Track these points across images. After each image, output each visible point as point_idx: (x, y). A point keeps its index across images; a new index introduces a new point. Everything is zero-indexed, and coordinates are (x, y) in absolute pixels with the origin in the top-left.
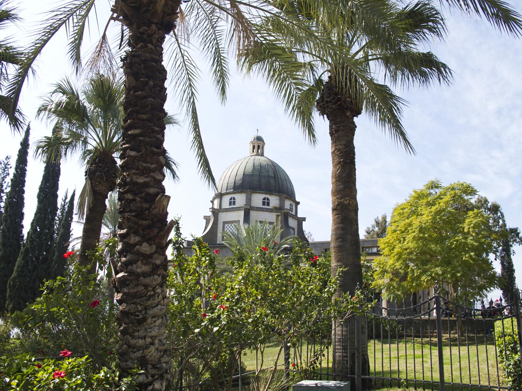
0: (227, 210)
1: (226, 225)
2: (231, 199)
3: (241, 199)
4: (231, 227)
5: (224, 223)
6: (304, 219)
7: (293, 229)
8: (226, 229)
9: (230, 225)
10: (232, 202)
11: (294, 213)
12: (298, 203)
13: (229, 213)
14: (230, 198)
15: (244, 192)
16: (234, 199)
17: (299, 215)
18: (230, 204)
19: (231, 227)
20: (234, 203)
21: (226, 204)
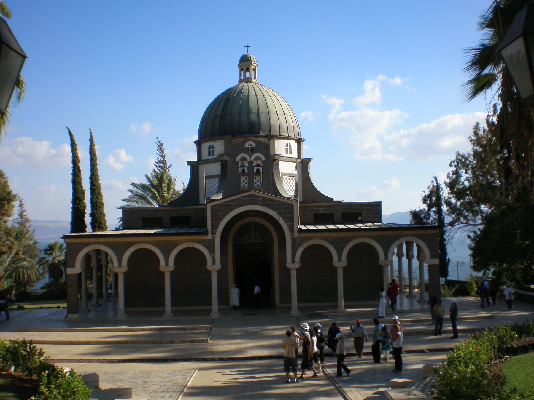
0: (208, 162)
2: (209, 148)
3: (219, 146)
4: (212, 183)
8: (208, 186)
9: (211, 181)
10: (211, 152)
11: (295, 154)
12: (299, 141)
14: (208, 146)
15: (222, 139)
16: (213, 147)
17: (304, 156)
18: (209, 155)
19: (212, 183)
20: (213, 154)
21: (205, 155)
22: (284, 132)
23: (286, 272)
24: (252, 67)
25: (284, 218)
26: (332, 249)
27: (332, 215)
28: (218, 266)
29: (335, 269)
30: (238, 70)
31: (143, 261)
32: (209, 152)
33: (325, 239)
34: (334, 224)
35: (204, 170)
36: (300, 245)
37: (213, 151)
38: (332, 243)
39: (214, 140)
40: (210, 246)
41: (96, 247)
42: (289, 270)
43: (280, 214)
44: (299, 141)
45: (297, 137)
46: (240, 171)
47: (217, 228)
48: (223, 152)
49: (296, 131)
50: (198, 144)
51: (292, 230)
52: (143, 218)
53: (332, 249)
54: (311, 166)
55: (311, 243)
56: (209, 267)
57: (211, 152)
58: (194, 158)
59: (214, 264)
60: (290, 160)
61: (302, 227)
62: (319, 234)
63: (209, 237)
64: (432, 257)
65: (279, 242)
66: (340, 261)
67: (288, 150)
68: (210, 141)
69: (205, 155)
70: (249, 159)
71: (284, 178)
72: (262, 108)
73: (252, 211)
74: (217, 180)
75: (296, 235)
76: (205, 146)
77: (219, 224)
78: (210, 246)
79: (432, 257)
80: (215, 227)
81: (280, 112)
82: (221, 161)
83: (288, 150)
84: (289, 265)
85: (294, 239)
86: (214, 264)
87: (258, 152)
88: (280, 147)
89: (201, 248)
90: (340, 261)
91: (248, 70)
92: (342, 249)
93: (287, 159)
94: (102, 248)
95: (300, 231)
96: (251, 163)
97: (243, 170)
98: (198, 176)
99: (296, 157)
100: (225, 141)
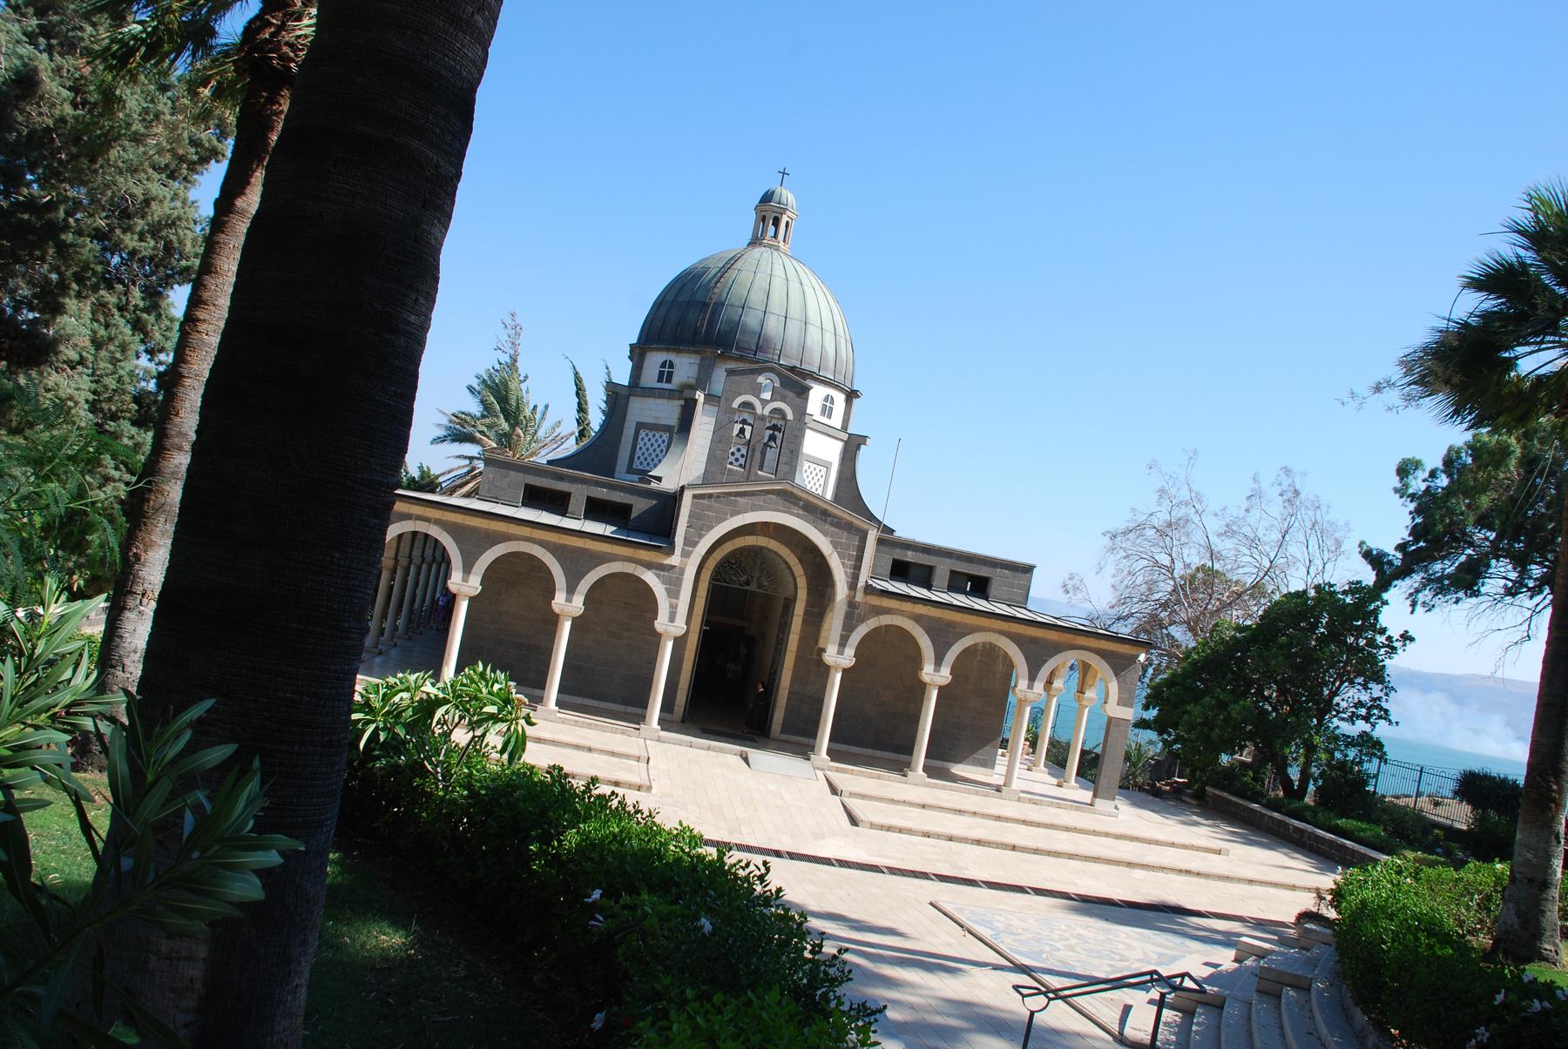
0: (651, 393)
1: (643, 433)
2: (663, 365)
3: (685, 367)
5: (640, 426)
6: (862, 440)
7: (827, 466)
10: (666, 374)
11: (836, 421)
12: (851, 395)
13: (650, 400)
16: (671, 365)
18: (660, 380)
20: (669, 381)
21: (650, 378)
22: (826, 369)
23: (813, 668)
24: (784, 219)
25: (841, 556)
27: (930, 570)
28: (679, 626)
29: (922, 687)
30: (751, 217)
31: (518, 581)
32: (661, 373)
33: (918, 619)
34: (929, 588)
35: (641, 410)
36: (862, 620)
37: (670, 375)
38: (929, 631)
39: (678, 351)
40: (673, 579)
41: (421, 527)
42: (827, 669)
43: (835, 545)
44: (851, 395)
46: (736, 432)
47: (695, 544)
48: (693, 381)
49: (849, 376)
50: (638, 353)
51: (853, 586)
52: (527, 485)
54: (863, 455)
55: (886, 620)
56: (661, 623)
57: (666, 374)
58: (622, 377)
59: (672, 618)
60: (827, 431)
62: (907, 606)
63: (674, 560)
64: (1123, 702)
65: (809, 604)
66: (936, 675)
67: (827, 411)
68: (668, 350)
69: (650, 378)
70: (759, 411)
71: (806, 465)
72: (795, 311)
73: (766, 524)
74: (666, 436)
75: (859, 597)
76: (654, 360)
77: (701, 537)
78: (673, 579)
79: (1123, 702)
80: (690, 542)
81: (828, 326)
82: (686, 400)
83: (827, 411)
84: (831, 655)
85: (851, 604)
86: (672, 618)
87: (783, 400)
89: (650, 578)
90: (936, 675)
91: (776, 222)
92: (949, 646)
93: (821, 428)
94: (435, 532)
95: (869, 589)
96: (762, 418)
97: (742, 431)
98: (624, 418)
100: (703, 359)
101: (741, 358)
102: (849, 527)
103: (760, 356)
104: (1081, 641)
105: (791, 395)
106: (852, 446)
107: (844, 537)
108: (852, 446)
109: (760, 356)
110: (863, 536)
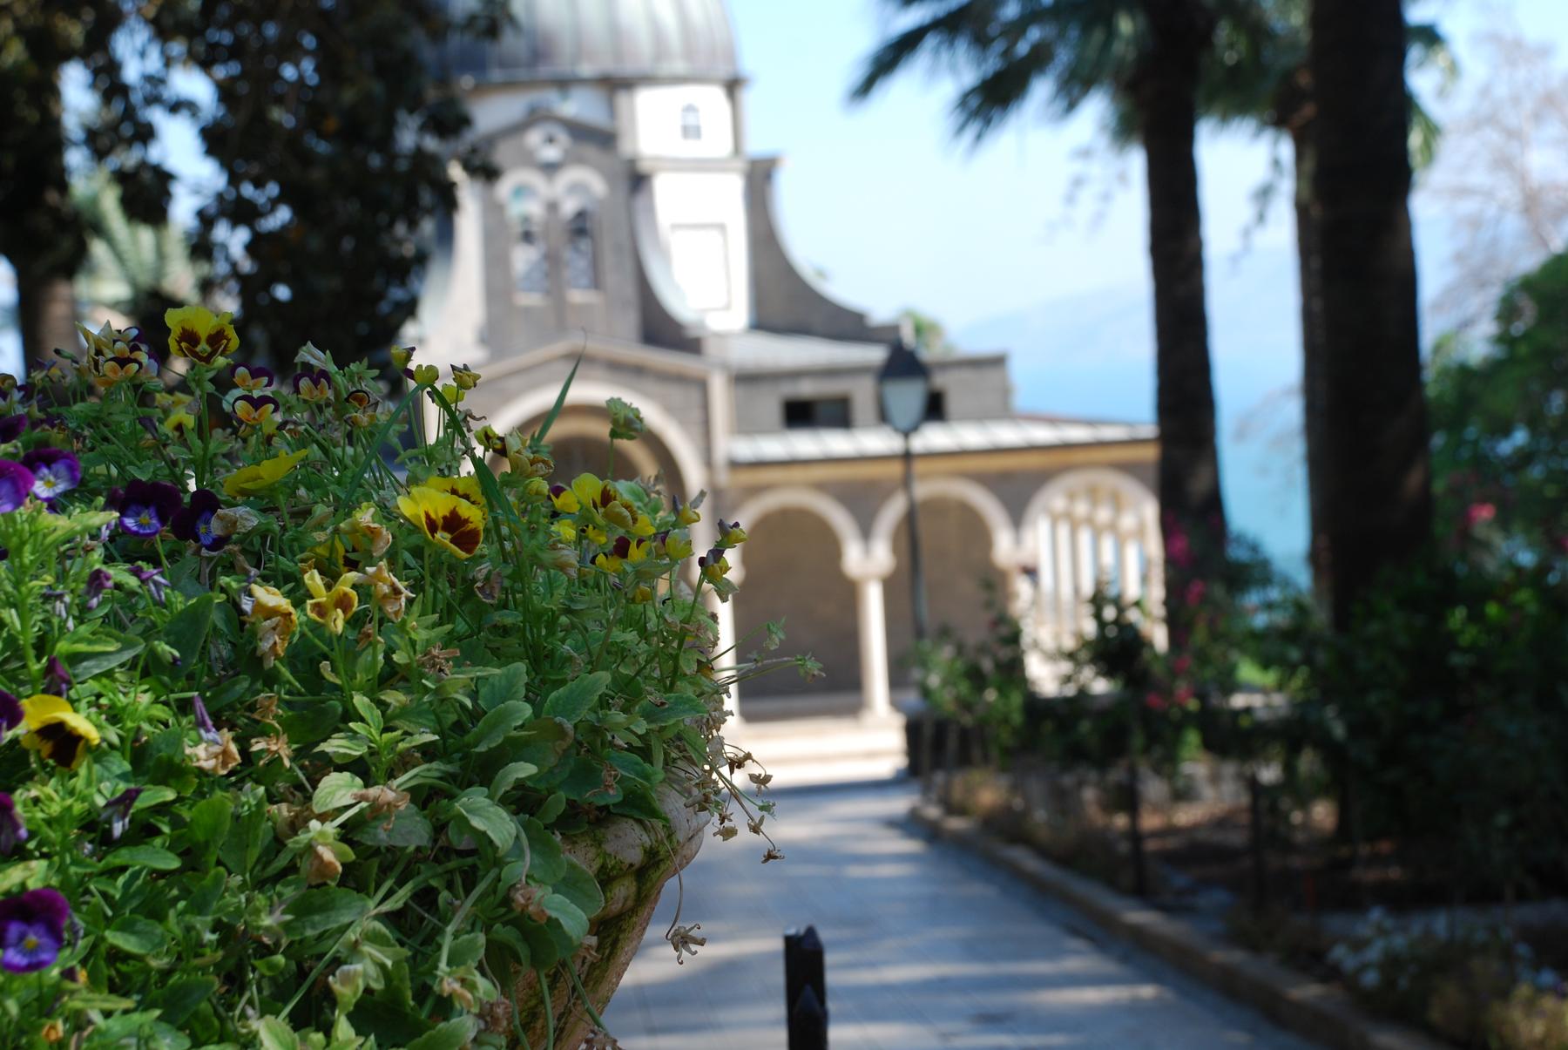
11: (717, 142)
12: (733, 86)
17: (757, 146)
26: (840, 519)
33: (821, 487)
43: (669, 409)
44: (733, 86)
45: (723, 71)
51: (708, 462)
53: (840, 519)
61: (746, 449)
62: (797, 474)
66: (868, 560)
88: (654, 123)
90: (868, 560)
95: (735, 465)
99: (724, 147)
101: (510, 85)
102: (680, 379)
103: (544, 71)
104: (1079, 456)
105: (590, 151)
106: (760, 178)
107: (676, 393)
108: (760, 178)
109: (544, 71)
110: (702, 385)
